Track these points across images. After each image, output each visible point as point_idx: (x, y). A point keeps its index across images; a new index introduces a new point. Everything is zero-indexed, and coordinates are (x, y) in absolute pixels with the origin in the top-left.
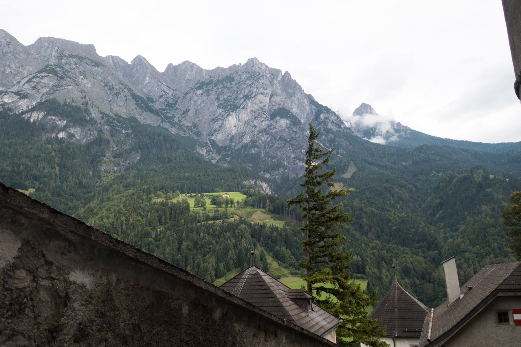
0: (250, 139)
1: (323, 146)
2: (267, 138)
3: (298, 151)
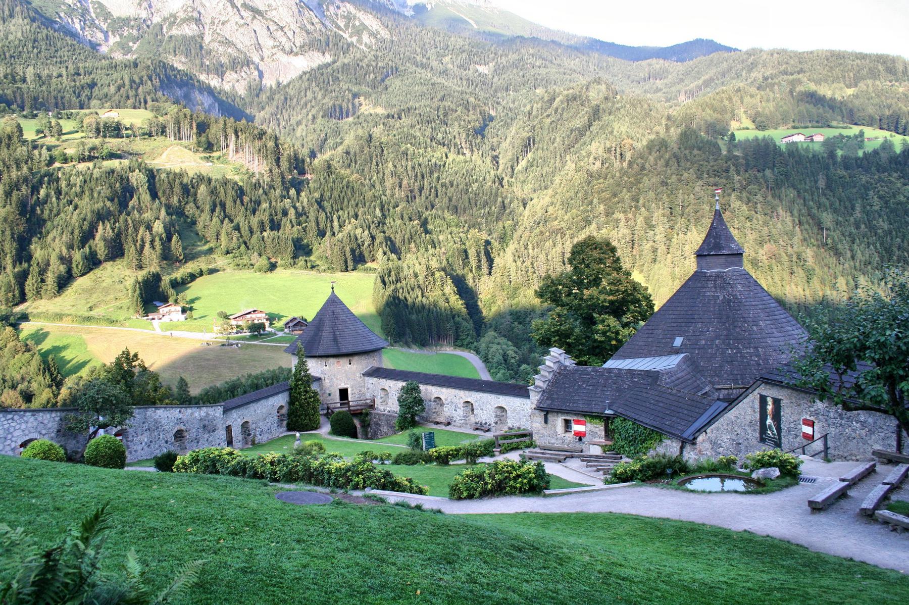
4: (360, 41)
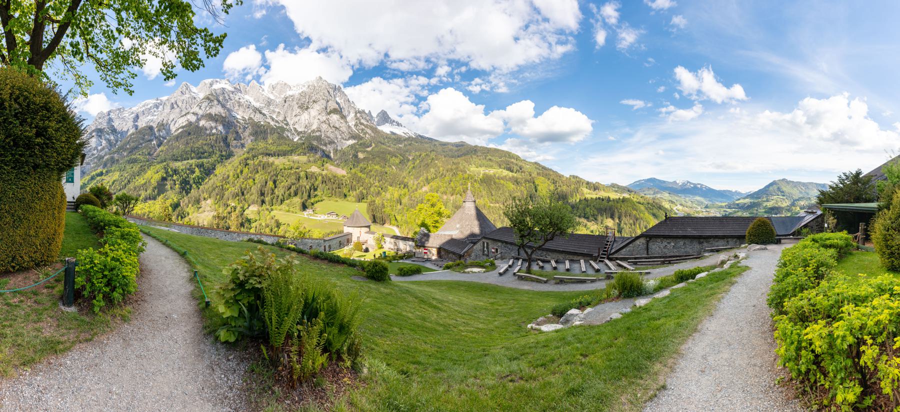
4: (366, 136)
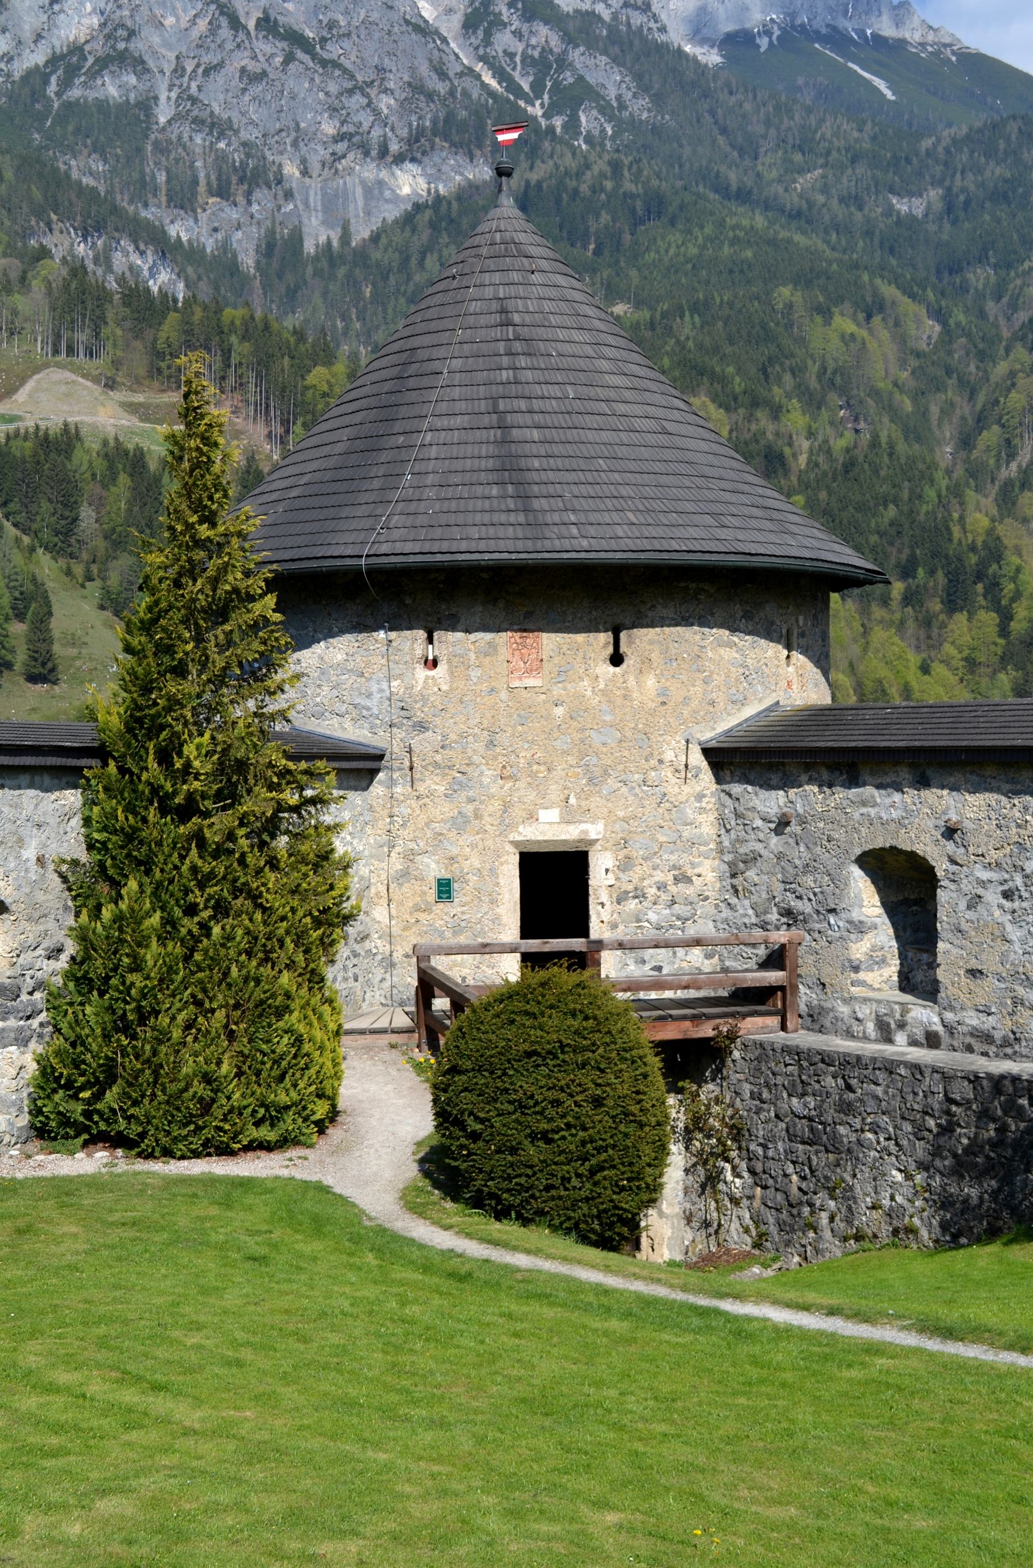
0: (95, 21)
1: (493, 83)
2: (193, 22)
3: (358, 100)
4: (572, 125)
